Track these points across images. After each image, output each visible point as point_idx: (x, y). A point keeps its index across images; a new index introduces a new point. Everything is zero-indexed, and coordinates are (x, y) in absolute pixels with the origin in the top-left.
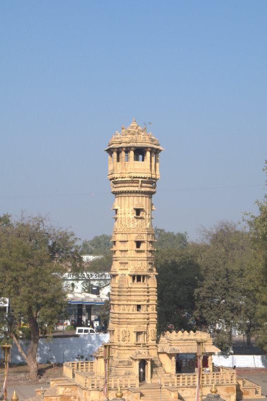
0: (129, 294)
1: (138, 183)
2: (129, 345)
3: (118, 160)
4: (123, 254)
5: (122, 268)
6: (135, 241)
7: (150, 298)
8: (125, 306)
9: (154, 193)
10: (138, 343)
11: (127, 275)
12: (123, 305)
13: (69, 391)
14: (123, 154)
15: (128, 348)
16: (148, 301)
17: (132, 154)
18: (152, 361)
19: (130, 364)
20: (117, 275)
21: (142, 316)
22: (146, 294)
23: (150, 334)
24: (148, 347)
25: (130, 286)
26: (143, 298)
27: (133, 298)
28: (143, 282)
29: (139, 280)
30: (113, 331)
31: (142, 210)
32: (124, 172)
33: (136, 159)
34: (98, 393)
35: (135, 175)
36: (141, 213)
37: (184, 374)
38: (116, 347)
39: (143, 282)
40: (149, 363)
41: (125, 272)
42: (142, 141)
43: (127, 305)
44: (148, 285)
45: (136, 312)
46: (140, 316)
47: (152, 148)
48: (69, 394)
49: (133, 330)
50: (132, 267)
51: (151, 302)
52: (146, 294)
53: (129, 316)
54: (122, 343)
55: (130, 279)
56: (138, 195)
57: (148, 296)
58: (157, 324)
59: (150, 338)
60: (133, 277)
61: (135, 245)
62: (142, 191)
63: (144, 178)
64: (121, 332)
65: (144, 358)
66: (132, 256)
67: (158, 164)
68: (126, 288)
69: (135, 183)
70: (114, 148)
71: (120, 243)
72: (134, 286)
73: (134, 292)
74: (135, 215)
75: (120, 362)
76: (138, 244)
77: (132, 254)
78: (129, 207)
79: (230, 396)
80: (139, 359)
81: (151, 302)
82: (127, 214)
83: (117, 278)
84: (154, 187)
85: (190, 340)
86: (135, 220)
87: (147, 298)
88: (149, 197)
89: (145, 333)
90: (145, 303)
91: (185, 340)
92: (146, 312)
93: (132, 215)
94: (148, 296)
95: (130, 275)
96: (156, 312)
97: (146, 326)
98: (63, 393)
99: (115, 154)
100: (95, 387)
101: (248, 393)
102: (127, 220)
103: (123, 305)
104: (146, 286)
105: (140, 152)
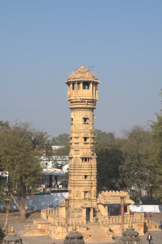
0: (80, 169)
1: (85, 102)
2: (80, 199)
3: (73, 89)
4: (76, 145)
5: (76, 153)
7: (93, 171)
8: (78, 176)
9: (95, 108)
10: (85, 198)
11: (79, 157)
12: (77, 175)
13: (45, 226)
14: (76, 85)
15: (80, 201)
16: (91, 173)
17: (81, 85)
18: (94, 209)
19: (80, 210)
20: (73, 158)
21: (87, 182)
22: (90, 169)
23: (93, 193)
24: (91, 200)
25: (80, 164)
26: (88, 171)
27: (82, 171)
28: (88, 161)
29: (86, 160)
31: (88, 118)
32: (77, 96)
33: (84, 88)
34: (61, 227)
35: (83, 98)
36: (87, 120)
37: (113, 216)
38: (73, 200)
39: (88, 161)
40: (92, 209)
41: (77, 156)
42: (87, 77)
43: (79, 175)
44: (91, 164)
45: (84, 179)
46: (87, 182)
47: (94, 82)
48: (45, 228)
49: (82, 190)
50: (82, 153)
51: (93, 174)
52: (90, 169)
53: (80, 182)
54: (76, 198)
55: (81, 160)
56: (86, 110)
57: (91, 170)
58: (96, 187)
59: (93, 195)
60: (83, 159)
61: (83, 139)
62: (88, 107)
63: (89, 99)
64: (75, 192)
65: (89, 207)
66: (82, 146)
67: (97, 91)
68: (78, 165)
69: (83, 102)
70: (71, 82)
71: (74, 138)
72: (83, 164)
73: (83, 167)
74: (83, 122)
75: (75, 209)
76: (85, 139)
77: (82, 145)
79: (140, 229)
80: (86, 208)
81: (93, 174)
82: (78, 121)
83: (73, 159)
84: (95, 105)
85: (116, 196)
87: (91, 171)
88: (92, 111)
89: (90, 192)
90: (90, 174)
92: (90, 180)
93: (82, 122)
94: (91, 170)
95: (81, 158)
96: (96, 180)
97: (90, 187)
99: (71, 85)
100: (60, 224)
101: (151, 228)
102: (78, 124)
103: (77, 175)
104: (90, 164)
105: (86, 84)
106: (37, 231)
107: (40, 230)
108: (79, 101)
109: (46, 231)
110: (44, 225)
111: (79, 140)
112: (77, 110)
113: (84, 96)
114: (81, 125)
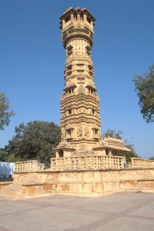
2: (89, 139)
4: (81, 73)
11: (84, 87)
30: (73, 129)
48: (50, 182)
49: (92, 127)
78: (82, 45)
86: (87, 54)
95: (86, 87)
98: (46, 181)
102: (82, 53)
106: (40, 188)
109: (54, 186)
110: (50, 176)
111: (83, 68)
112: (79, 38)
114: (84, 53)
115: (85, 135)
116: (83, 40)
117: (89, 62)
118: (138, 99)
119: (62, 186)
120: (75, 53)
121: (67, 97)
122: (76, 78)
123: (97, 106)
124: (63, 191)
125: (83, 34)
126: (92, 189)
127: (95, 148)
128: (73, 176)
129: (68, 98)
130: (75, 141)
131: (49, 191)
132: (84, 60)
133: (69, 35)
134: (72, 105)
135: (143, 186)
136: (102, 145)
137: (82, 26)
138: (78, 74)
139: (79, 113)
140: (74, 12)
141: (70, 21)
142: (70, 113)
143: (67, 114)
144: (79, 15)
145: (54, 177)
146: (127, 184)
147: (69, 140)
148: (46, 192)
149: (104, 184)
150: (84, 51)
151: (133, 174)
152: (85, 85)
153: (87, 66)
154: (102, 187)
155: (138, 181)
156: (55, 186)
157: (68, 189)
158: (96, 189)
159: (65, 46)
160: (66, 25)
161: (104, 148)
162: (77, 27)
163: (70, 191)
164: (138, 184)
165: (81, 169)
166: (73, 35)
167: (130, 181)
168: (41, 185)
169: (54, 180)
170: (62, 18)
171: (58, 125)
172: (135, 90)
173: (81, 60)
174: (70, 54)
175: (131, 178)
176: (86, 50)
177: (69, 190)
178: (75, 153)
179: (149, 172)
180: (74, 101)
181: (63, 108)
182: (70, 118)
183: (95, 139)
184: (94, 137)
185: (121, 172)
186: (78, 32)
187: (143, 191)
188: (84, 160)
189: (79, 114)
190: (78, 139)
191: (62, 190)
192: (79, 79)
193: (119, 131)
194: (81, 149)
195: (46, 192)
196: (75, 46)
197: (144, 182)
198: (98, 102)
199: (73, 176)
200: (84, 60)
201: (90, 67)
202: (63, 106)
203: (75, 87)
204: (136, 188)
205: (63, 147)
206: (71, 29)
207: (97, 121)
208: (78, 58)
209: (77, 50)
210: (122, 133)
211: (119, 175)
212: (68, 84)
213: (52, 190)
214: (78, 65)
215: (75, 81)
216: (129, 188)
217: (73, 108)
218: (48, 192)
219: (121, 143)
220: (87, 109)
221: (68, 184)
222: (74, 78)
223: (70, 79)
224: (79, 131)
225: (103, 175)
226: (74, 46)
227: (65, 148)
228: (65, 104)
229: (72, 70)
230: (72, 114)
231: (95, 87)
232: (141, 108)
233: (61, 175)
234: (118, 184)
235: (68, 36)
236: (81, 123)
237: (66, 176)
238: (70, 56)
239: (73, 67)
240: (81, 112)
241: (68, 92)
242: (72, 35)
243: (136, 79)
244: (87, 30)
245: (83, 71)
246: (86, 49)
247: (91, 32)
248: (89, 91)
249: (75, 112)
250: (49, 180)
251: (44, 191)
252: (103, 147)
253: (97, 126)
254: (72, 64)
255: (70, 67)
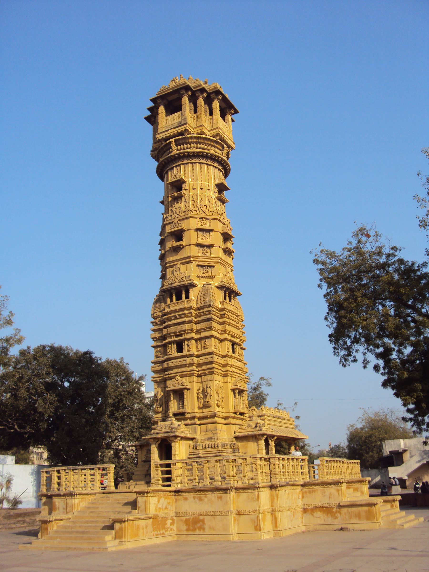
2: (225, 415)
6: (222, 234)
8: (217, 340)
12: (216, 338)
17: (216, 105)
25: (220, 306)
43: (219, 339)
49: (230, 386)
50: (221, 275)
61: (221, 239)
66: (220, 256)
74: (217, 195)
86: (219, 203)
91: (275, 417)
95: (220, 288)
98: (156, 511)
102: (207, 200)
107: (155, 518)
108: (209, 139)
109: (169, 522)
110: (162, 499)
112: (201, 161)
113: (223, 132)
115: (217, 404)
116: (210, 165)
117: (224, 224)
118: (324, 307)
119: (187, 522)
120: (191, 198)
121: (172, 309)
122: (195, 264)
123: (241, 334)
124: (190, 533)
125: (213, 151)
126: (256, 524)
127: (240, 434)
128: (213, 499)
129: (175, 311)
130: (193, 418)
131: (161, 532)
132: (214, 219)
133: (175, 150)
134: (184, 332)
135: (350, 517)
136: (257, 429)
137: (209, 131)
138: (199, 255)
139: (203, 351)
140: (190, 93)
141: (179, 113)
142: (180, 349)
143: (172, 350)
144: (201, 101)
145: (168, 503)
146: (318, 514)
147: (180, 416)
148: (157, 535)
149: (278, 515)
150: (213, 194)
151: (330, 494)
152: (215, 283)
153: (220, 235)
154: (274, 521)
155: (340, 506)
156: (171, 521)
157: (202, 528)
158: (264, 524)
159: (162, 173)
160: (167, 122)
161: (263, 435)
162: (197, 134)
163: (207, 531)
164: (340, 513)
165: (232, 486)
166: (188, 153)
167: (323, 507)
168: (150, 518)
169: (169, 509)
170: (159, 101)
171: (100, 359)
172: (319, 286)
173: (206, 219)
174: (177, 199)
175: (325, 501)
176: (217, 192)
177: (204, 529)
178: (195, 447)
179: (356, 490)
180: (191, 322)
181: (157, 335)
182: (180, 363)
183: (238, 413)
184: (236, 410)
185: (306, 489)
186: (199, 146)
187: (349, 527)
188: (235, 466)
189: (204, 355)
190: (198, 413)
191: (187, 530)
192: (202, 266)
193: (262, 378)
194: (209, 439)
195: (157, 535)
196: (190, 179)
197: (354, 509)
198: (243, 321)
199: (213, 499)
200: (212, 219)
201: (227, 237)
202: (160, 330)
203: (193, 286)
204: (336, 521)
205: (171, 434)
206: (182, 137)
207: (241, 369)
208: (199, 214)
209: (194, 192)
210: (269, 384)
211: (300, 496)
212: (175, 278)
213: (166, 531)
214: (197, 230)
215: (191, 272)
216: (322, 522)
217: (189, 339)
218: (160, 534)
219: (287, 420)
220: (222, 341)
221: (201, 518)
222: (189, 262)
223: (179, 265)
224: (201, 396)
225: (275, 497)
226: (189, 181)
227: (176, 437)
228: (165, 327)
229: (184, 243)
230: (184, 353)
231: (236, 288)
232: (331, 331)
233: (182, 499)
234: (300, 514)
235: (172, 154)
236: (209, 377)
237: (196, 499)
238: (177, 205)
239: (185, 235)
240: (208, 351)
241: (174, 298)
242: (185, 152)
243: (322, 258)
244: (220, 141)
245: (210, 246)
246: (217, 190)
247: (229, 147)
248: (225, 299)
249: (193, 348)
250: (160, 508)
251: (153, 532)
252: (259, 435)
253: (243, 383)
254: (184, 225)
255: (178, 235)
